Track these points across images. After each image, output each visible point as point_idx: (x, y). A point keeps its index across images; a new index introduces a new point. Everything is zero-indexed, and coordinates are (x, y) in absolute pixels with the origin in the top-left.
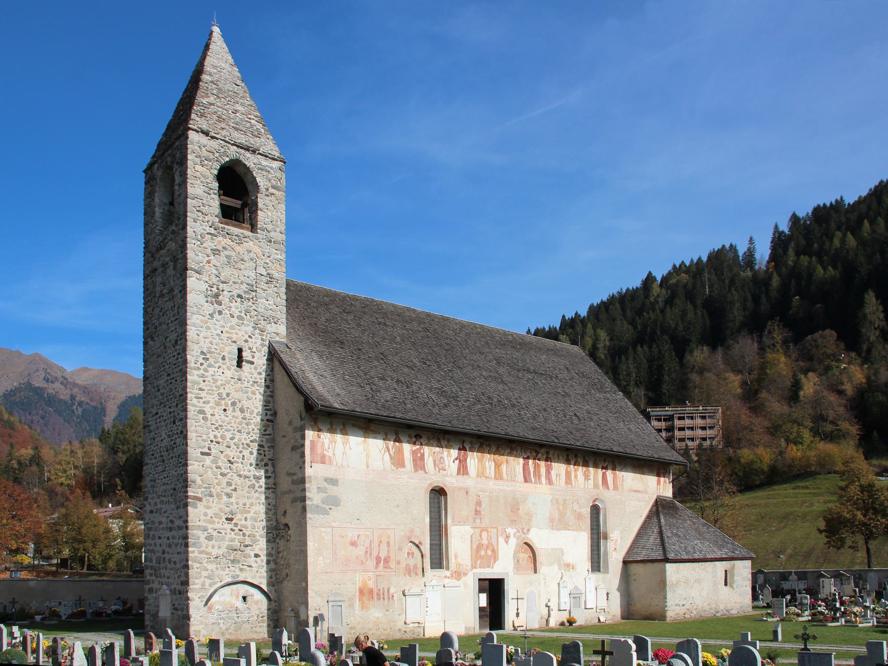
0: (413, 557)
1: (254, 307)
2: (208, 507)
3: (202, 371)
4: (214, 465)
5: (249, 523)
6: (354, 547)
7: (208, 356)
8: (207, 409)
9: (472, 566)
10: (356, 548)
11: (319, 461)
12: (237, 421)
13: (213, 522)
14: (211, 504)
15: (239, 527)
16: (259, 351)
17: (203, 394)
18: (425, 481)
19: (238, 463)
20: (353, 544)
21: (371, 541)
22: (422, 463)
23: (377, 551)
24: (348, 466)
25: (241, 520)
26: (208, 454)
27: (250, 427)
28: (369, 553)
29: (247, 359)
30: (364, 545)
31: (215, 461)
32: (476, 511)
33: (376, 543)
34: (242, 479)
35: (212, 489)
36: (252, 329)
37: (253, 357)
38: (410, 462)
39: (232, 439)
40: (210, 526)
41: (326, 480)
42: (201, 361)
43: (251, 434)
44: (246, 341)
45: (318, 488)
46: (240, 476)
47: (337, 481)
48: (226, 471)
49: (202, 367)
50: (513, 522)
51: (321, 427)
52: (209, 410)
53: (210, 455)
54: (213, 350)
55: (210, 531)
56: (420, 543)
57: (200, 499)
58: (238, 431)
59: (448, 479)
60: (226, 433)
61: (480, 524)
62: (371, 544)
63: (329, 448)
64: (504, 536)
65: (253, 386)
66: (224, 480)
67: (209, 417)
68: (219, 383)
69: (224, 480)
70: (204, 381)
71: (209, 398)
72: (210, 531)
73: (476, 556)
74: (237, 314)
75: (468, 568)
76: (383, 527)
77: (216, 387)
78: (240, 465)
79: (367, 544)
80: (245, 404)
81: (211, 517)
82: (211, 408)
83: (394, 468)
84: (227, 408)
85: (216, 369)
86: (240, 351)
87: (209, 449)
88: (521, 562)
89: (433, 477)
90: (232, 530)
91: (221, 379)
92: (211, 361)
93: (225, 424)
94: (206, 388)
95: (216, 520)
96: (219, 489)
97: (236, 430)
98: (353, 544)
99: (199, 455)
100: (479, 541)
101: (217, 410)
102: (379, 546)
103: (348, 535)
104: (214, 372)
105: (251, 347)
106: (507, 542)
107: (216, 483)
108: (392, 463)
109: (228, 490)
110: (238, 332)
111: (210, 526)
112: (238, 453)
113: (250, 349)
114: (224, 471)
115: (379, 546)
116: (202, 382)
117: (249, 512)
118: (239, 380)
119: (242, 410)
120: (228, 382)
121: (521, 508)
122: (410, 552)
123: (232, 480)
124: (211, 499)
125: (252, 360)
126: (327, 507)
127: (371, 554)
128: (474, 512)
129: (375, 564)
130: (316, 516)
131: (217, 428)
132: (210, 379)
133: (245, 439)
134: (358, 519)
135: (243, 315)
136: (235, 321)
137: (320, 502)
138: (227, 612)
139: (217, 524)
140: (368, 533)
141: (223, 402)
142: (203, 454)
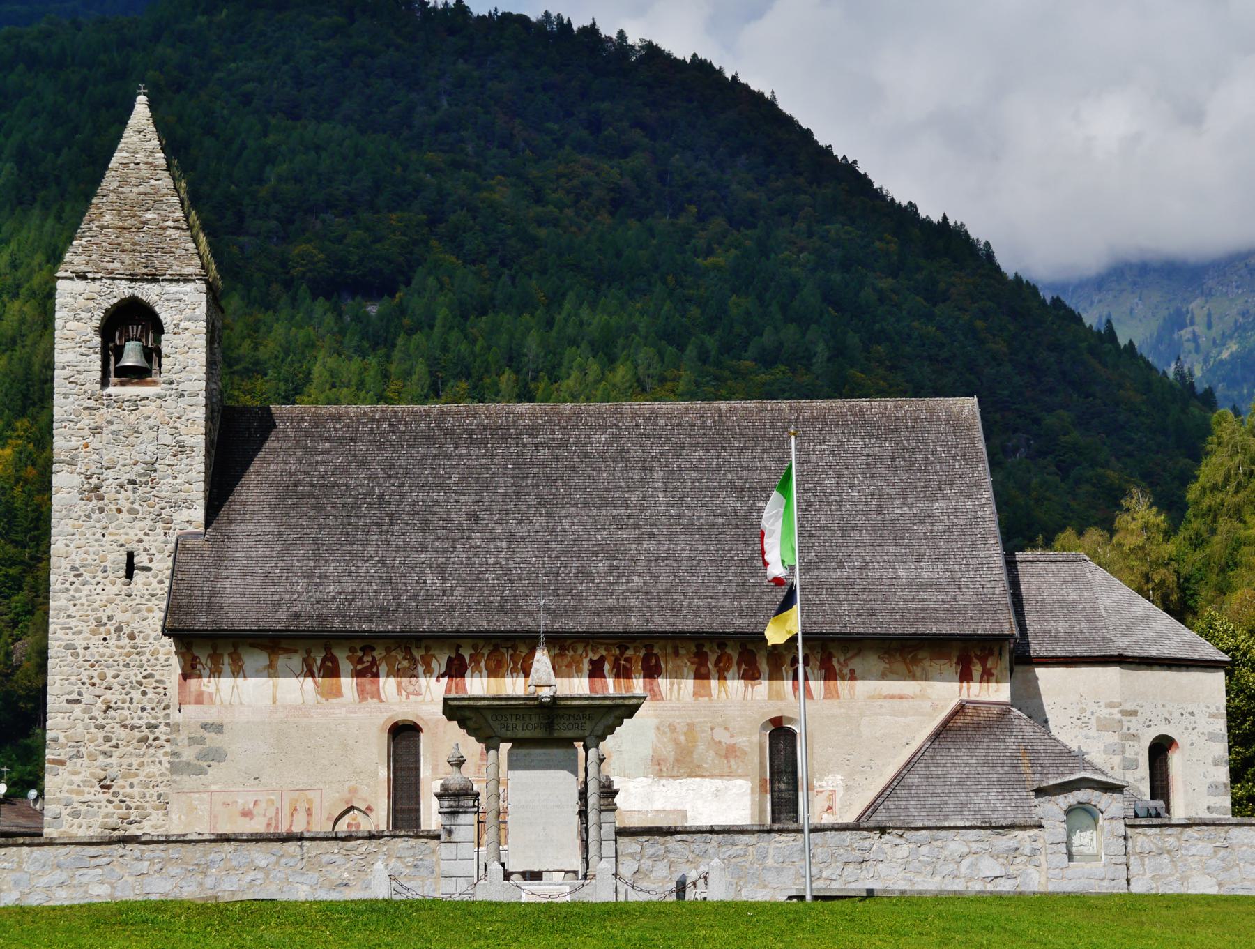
1: (155, 492)
2: (75, 773)
3: (72, 593)
4: (87, 716)
5: (136, 791)
6: (248, 819)
7: (82, 570)
8: (79, 642)
10: (251, 819)
11: (193, 701)
12: (125, 651)
14: (78, 768)
15: (120, 797)
16: (161, 551)
17: (72, 623)
19: (123, 708)
21: (277, 809)
22: (374, 688)
24: (241, 703)
25: (124, 787)
26: (77, 702)
27: (144, 658)
29: (141, 565)
30: (265, 815)
31: (85, 711)
33: (287, 810)
34: (128, 730)
35: (83, 749)
36: (151, 523)
37: (151, 561)
38: (352, 687)
39: (116, 677)
40: (75, 798)
42: (72, 579)
43: (145, 667)
44: (141, 541)
46: (125, 726)
47: (222, 726)
48: (104, 722)
49: (72, 588)
51: (196, 654)
52: (81, 642)
53: (81, 702)
54: (90, 561)
55: (76, 804)
56: (369, 808)
57: (62, 763)
58: (124, 666)
59: (424, 707)
60: (106, 670)
62: (277, 813)
65: (149, 600)
66: (100, 735)
67: (81, 651)
68: (96, 605)
69: (100, 735)
70: (75, 605)
72: (76, 804)
74: (123, 503)
76: (300, 787)
77: (93, 610)
78: (126, 712)
79: (271, 812)
80: (136, 626)
81: (79, 786)
82: (85, 639)
83: (323, 700)
84: (108, 637)
85: (92, 587)
86: (130, 556)
87: (80, 694)
89: (396, 708)
90: (110, 802)
91: (100, 599)
92: (86, 576)
93: (105, 658)
94: (77, 615)
95: (87, 789)
96: (92, 747)
97: (121, 663)
99: (65, 704)
102: (292, 815)
104: (90, 591)
105: (148, 548)
108: (318, 693)
109: (106, 747)
110: (129, 531)
111: (75, 798)
112: (124, 696)
113: (146, 550)
114: (101, 721)
115: (292, 815)
116: (72, 607)
117: (136, 775)
118: (130, 596)
119: (132, 637)
120: (110, 602)
123: (113, 733)
124: (80, 761)
125: (149, 565)
126: (204, 764)
130: (185, 777)
131: (92, 666)
132: (84, 600)
133: (136, 675)
135: (136, 506)
136: (125, 516)
139: (86, 795)
140: (273, 798)
141: (102, 629)
142: (69, 701)
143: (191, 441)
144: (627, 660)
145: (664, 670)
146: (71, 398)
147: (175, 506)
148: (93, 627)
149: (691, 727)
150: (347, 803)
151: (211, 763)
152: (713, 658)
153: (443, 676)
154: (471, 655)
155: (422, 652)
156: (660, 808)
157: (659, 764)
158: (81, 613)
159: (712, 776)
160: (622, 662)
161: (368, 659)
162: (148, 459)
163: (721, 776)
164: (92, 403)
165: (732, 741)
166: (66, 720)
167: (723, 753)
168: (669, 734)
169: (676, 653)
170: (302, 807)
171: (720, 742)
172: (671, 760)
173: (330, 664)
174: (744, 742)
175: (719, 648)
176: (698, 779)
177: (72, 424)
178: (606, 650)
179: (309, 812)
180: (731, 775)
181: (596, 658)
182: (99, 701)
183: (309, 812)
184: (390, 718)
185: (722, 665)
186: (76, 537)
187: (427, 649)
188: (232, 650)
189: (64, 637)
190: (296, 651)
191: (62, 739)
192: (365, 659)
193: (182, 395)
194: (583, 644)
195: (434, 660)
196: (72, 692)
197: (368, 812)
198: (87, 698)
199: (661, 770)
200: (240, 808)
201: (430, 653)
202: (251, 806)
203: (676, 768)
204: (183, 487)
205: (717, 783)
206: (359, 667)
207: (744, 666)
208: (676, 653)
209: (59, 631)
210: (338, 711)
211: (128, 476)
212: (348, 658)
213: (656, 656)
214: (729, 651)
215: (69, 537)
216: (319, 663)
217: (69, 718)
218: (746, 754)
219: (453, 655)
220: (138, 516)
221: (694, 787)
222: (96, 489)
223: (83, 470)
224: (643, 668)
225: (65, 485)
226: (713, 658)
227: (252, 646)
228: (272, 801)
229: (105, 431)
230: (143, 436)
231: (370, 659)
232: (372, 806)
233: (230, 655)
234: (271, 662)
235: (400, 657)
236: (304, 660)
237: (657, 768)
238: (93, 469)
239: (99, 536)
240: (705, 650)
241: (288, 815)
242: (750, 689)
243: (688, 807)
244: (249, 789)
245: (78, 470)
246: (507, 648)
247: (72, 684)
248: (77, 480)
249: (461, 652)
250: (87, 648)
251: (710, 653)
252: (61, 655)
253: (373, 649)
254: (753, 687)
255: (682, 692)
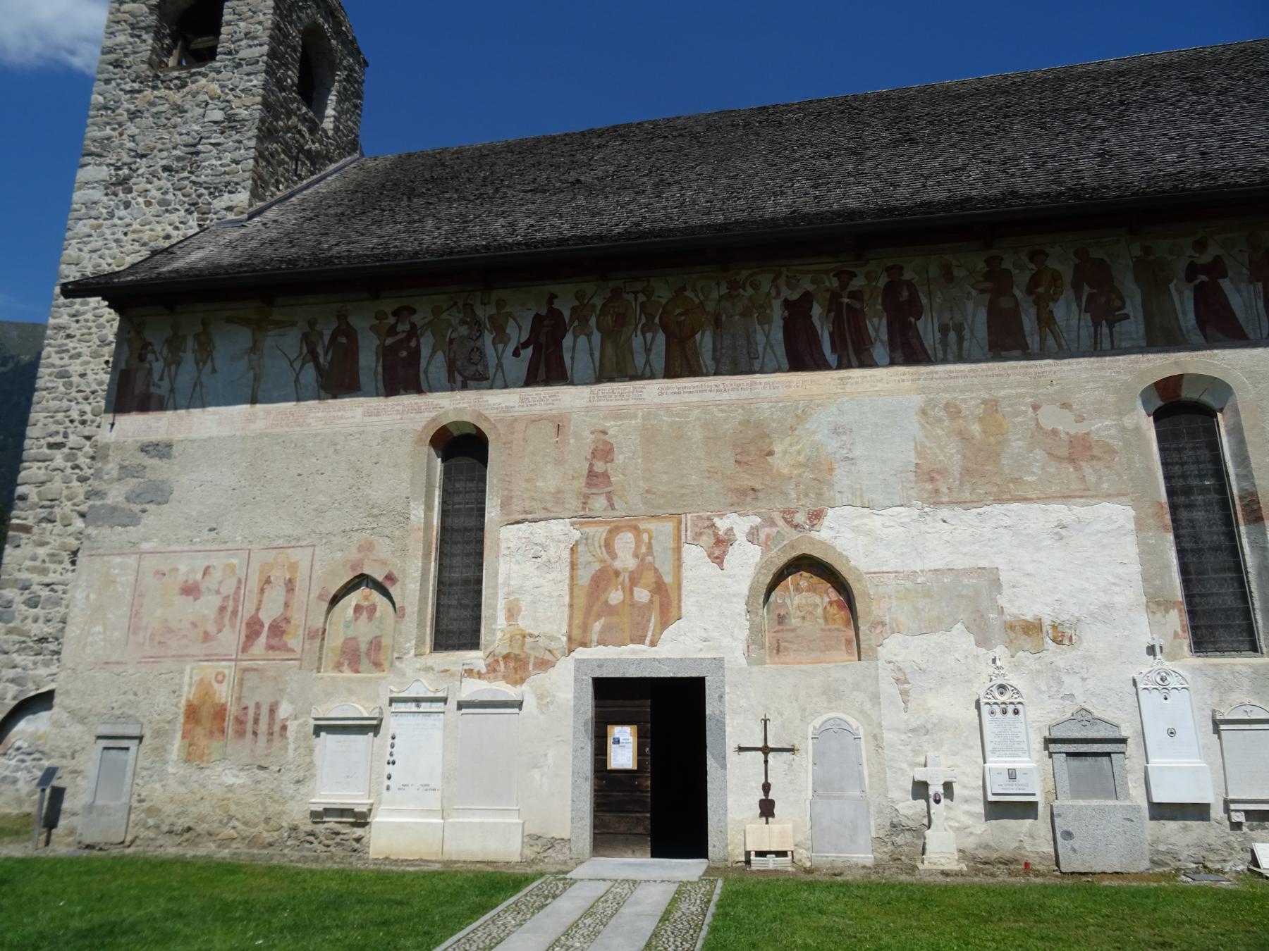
0: (370, 618)
2: (42, 544)
4: (69, 464)
6: (191, 598)
8: (75, 367)
9: (570, 639)
10: (196, 599)
13: (44, 571)
14: (48, 538)
17: (71, 344)
18: (418, 416)
20: (190, 590)
21: (239, 581)
23: (254, 607)
26: (59, 446)
28: (230, 609)
32: (591, 474)
33: (254, 583)
41: (145, 449)
45: (122, 467)
47: (169, 446)
50: (743, 497)
51: (149, 339)
55: (35, 588)
56: (390, 578)
57: (26, 529)
61: (611, 513)
62: (239, 588)
63: (161, 379)
64: (707, 540)
67: (75, 379)
68: (102, 320)
71: (83, 348)
73: (589, 608)
75: (553, 645)
76: (280, 542)
82: (83, 364)
88: (795, 622)
94: (78, 333)
95: (52, 566)
98: (190, 590)
99: (46, 451)
100: (602, 561)
101: (92, 366)
102: (262, 591)
103: (176, 570)
106: (719, 560)
107: (66, 497)
111: (36, 578)
115: (262, 591)
116: (74, 325)
121: (778, 448)
122: (366, 604)
124: (50, 525)
126: (136, 508)
127: (235, 613)
128: (583, 481)
129: (243, 639)
130: (106, 531)
132: (89, 316)
134: (212, 530)
135: (170, 197)
136: (156, 208)
137: (121, 499)
138: (37, 755)
139: (51, 575)
140: (235, 561)
143: (244, 113)
144: (855, 295)
145: (927, 309)
146: (113, 83)
147: (215, 191)
148: (94, 347)
149: (992, 406)
150: (353, 568)
151: (147, 506)
152: (1022, 278)
153: (525, 345)
154: (574, 310)
155: (492, 310)
156: (940, 565)
157: (932, 480)
158: (85, 331)
159: (1047, 499)
160: (846, 300)
161: (403, 327)
162: (191, 141)
163: (1066, 497)
164: (136, 86)
165: (1081, 429)
166: (43, 471)
167: (1064, 452)
168: (946, 423)
169: (948, 276)
170: (278, 576)
171: (1055, 432)
172: (956, 470)
173: (344, 340)
174: (1108, 428)
175: (1031, 260)
176: (1016, 506)
177: (109, 112)
178: (813, 281)
179: (290, 586)
180: (1088, 494)
181: (795, 296)
182: (88, 443)
183: (290, 586)
184: (434, 420)
185: (1041, 290)
186: (95, 238)
187: (500, 304)
188: (199, 329)
189: (58, 362)
190: (293, 324)
191: (33, 497)
192: (400, 328)
193: (239, 65)
194: (771, 276)
195: (511, 321)
196: (57, 433)
197: (387, 585)
198: (73, 440)
199: (937, 491)
200: (181, 578)
201: (507, 310)
202: (199, 576)
203: (967, 486)
204: (227, 169)
205: (1059, 511)
206: (389, 341)
207: (1087, 290)
208: (948, 276)
209: (53, 355)
210: (349, 414)
211: (164, 162)
212: (373, 328)
213: (910, 284)
214: (1052, 264)
215: (85, 239)
216: (327, 339)
217: (46, 468)
218: (1115, 452)
219: (543, 312)
220: (169, 208)
221: (1009, 522)
222: (126, 179)
223: (112, 162)
224: (885, 308)
225: (91, 179)
226: (1022, 278)
227: (229, 320)
228: (233, 567)
229: (146, 115)
230: (188, 115)
231: (407, 327)
232: (396, 574)
233: (196, 336)
234: (255, 343)
235: (455, 322)
236: (305, 337)
237: (929, 486)
238: (126, 159)
239: (120, 235)
240: (1004, 266)
241: (256, 590)
242: (1105, 330)
243: (999, 562)
244: (195, 548)
245: (109, 161)
246: (636, 293)
247: (58, 423)
248: (104, 173)
249: (557, 304)
250: (83, 375)
251: (1015, 271)
252: (50, 385)
253: (413, 311)
254: (1111, 327)
255: (966, 344)
